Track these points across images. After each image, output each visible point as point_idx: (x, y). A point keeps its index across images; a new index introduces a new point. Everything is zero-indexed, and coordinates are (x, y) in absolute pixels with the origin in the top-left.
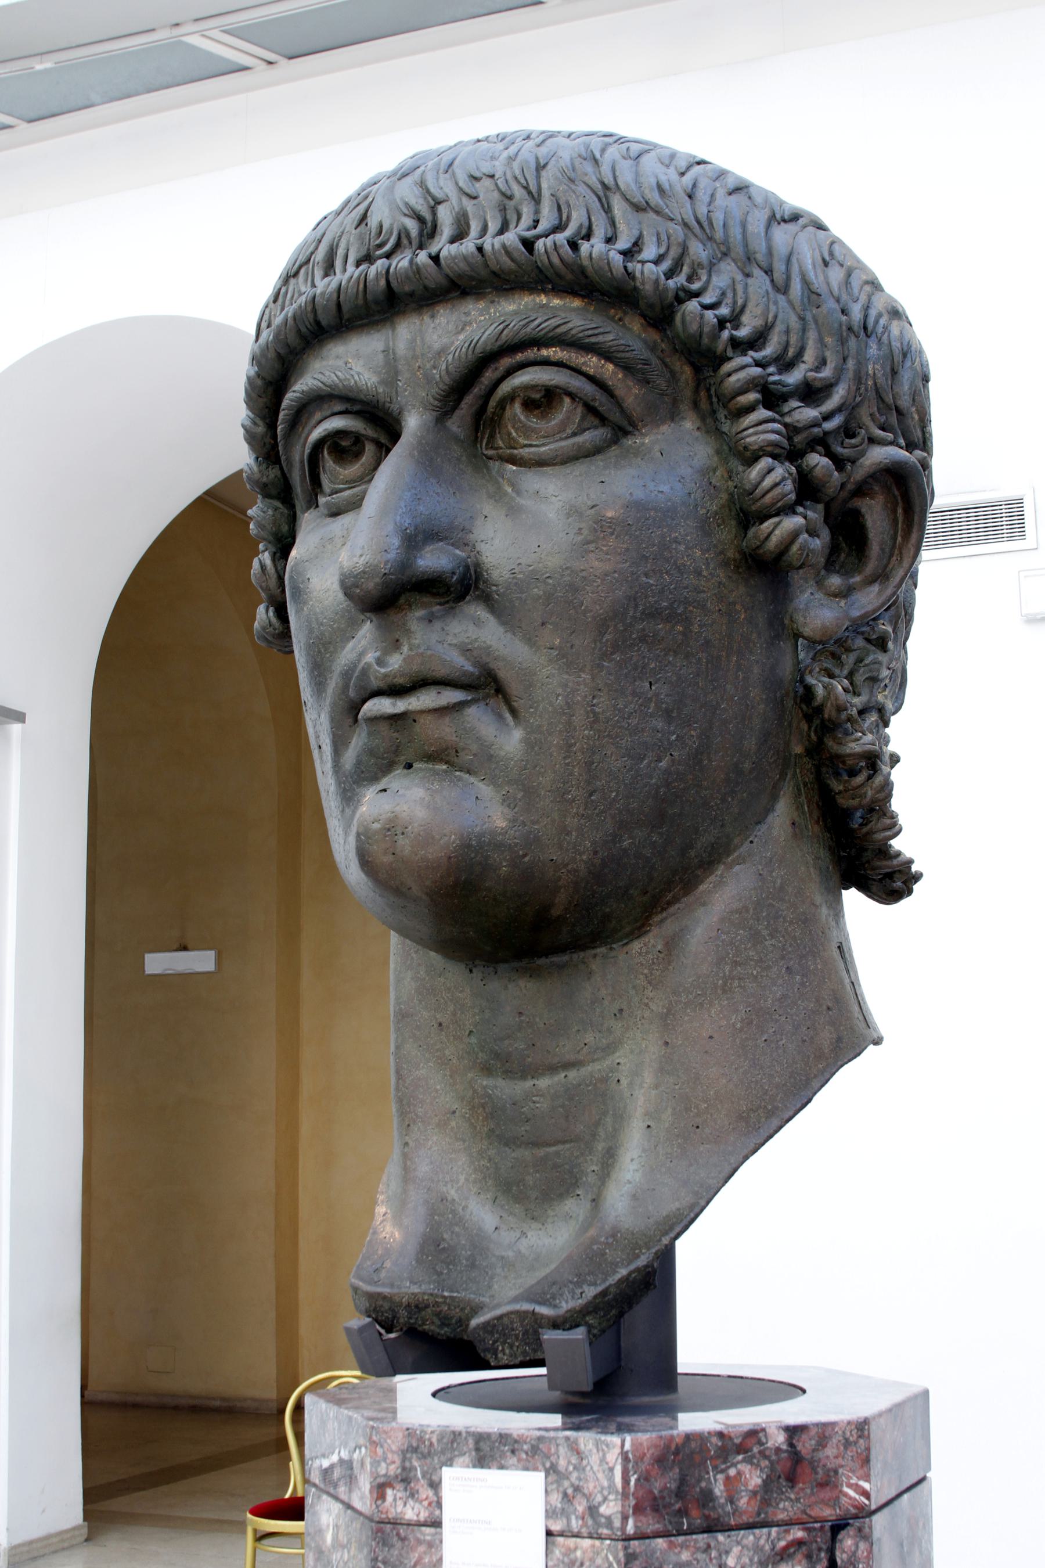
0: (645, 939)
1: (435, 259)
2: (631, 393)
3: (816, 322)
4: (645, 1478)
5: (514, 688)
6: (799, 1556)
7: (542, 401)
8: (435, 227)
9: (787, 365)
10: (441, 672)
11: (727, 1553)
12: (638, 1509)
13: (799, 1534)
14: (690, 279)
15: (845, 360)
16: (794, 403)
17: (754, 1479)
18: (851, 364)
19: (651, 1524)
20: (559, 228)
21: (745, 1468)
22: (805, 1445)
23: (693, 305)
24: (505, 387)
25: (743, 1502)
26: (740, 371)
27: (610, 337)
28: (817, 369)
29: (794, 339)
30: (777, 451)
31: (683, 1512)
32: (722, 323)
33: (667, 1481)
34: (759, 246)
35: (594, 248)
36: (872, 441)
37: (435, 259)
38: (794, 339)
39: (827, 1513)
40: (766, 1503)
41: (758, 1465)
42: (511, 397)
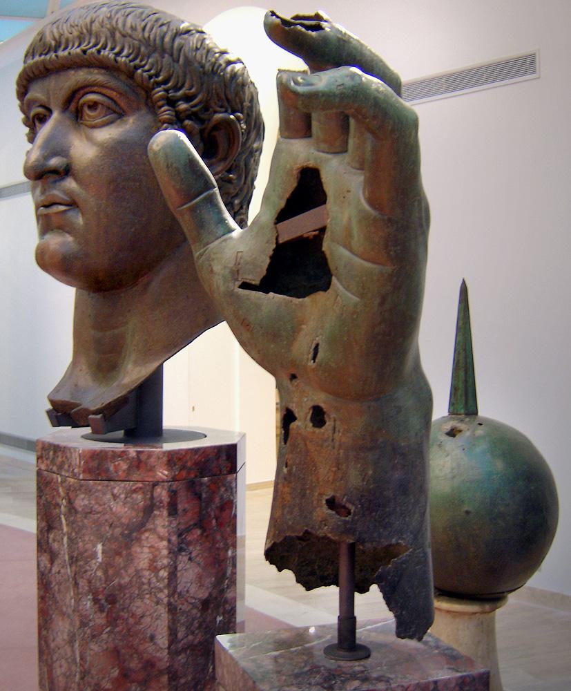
1: (57, 56)
2: (123, 104)
3: (190, 72)
4: (86, 462)
6: (140, 492)
9: (177, 88)
11: (115, 488)
12: (84, 472)
13: (140, 485)
14: (141, 61)
15: (202, 85)
16: (180, 103)
17: (125, 467)
18: (205, 85)
19: (88, 476)
20: (95, 45)
21: (121, 462)
22: (143, 457)
23: (139, 71)
25: (120, 473)
26: (159, 92)
27: (111, 84)
28: (190, 89)
29: (180, 79)
30: (170, 121)
31: (99, 474)
32: (150, 77)
33: (94, 464)
34: (167, 46)
35: (105, 53)
36: (216, 112)
37: (57, 56)
38: (180, 79)
39: (151, 479)
40: (128, 474)
41: (126, 462)
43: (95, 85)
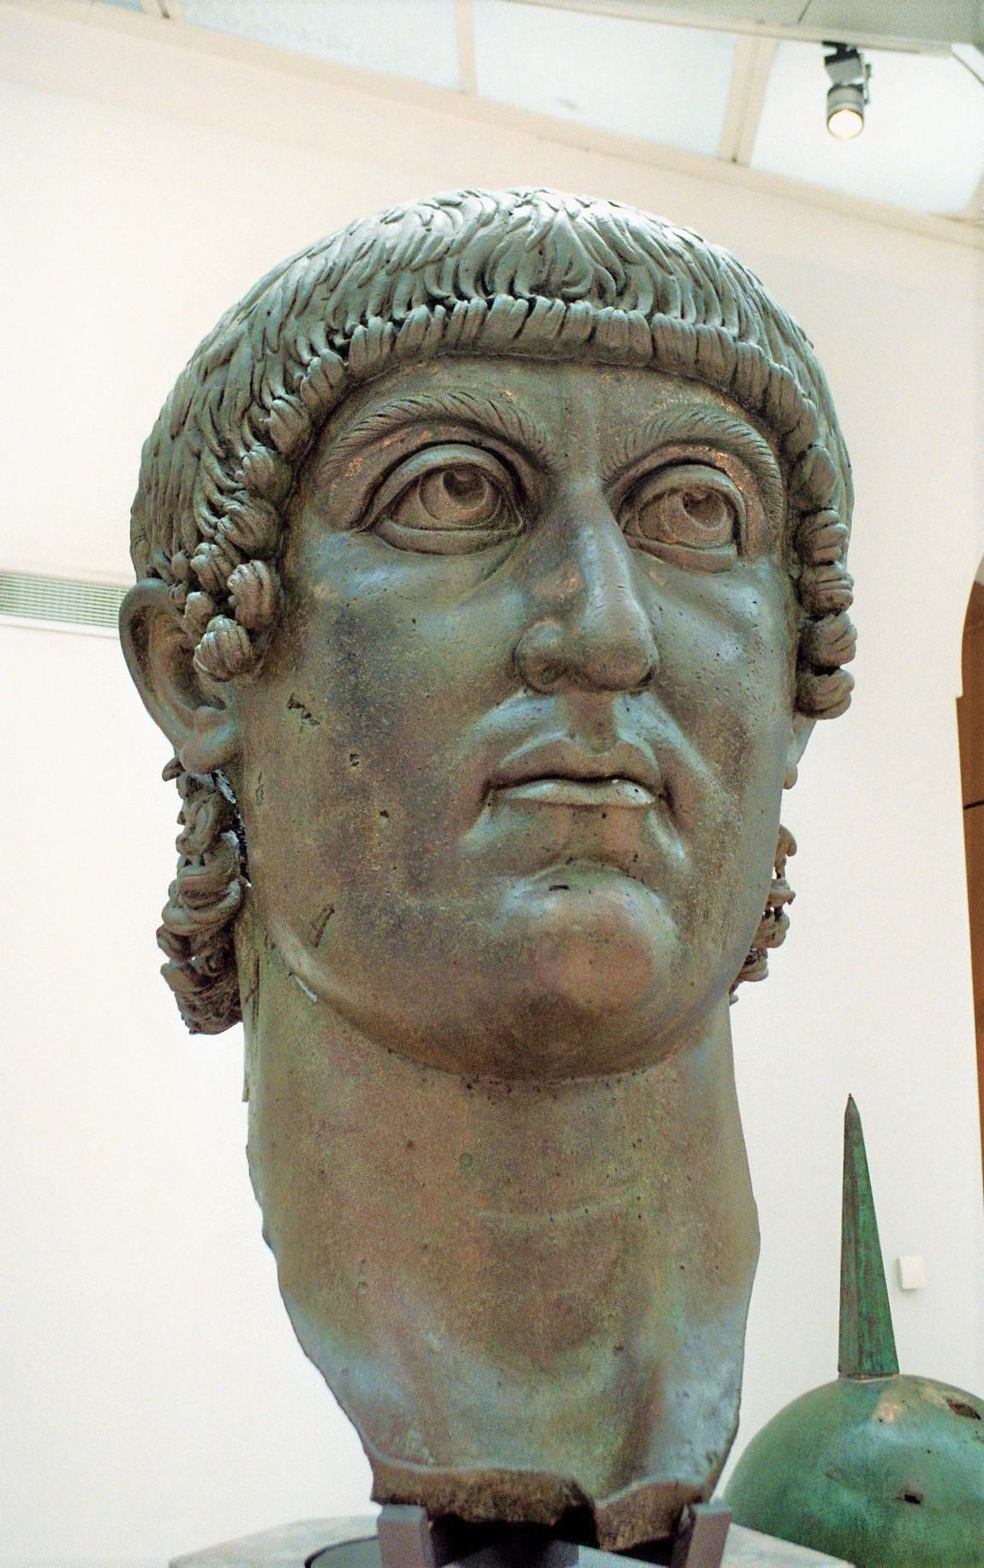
0: (662, 1066)
5: (683, 800)
7: (702, 503)
8: (626, 286)
10: (637, 770)
24: (676, 478)
42: (674, 491)
43: (714, 444)
